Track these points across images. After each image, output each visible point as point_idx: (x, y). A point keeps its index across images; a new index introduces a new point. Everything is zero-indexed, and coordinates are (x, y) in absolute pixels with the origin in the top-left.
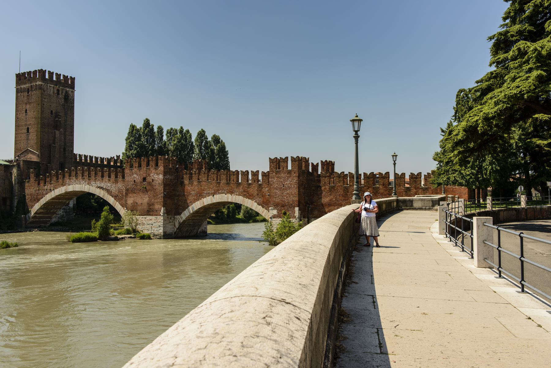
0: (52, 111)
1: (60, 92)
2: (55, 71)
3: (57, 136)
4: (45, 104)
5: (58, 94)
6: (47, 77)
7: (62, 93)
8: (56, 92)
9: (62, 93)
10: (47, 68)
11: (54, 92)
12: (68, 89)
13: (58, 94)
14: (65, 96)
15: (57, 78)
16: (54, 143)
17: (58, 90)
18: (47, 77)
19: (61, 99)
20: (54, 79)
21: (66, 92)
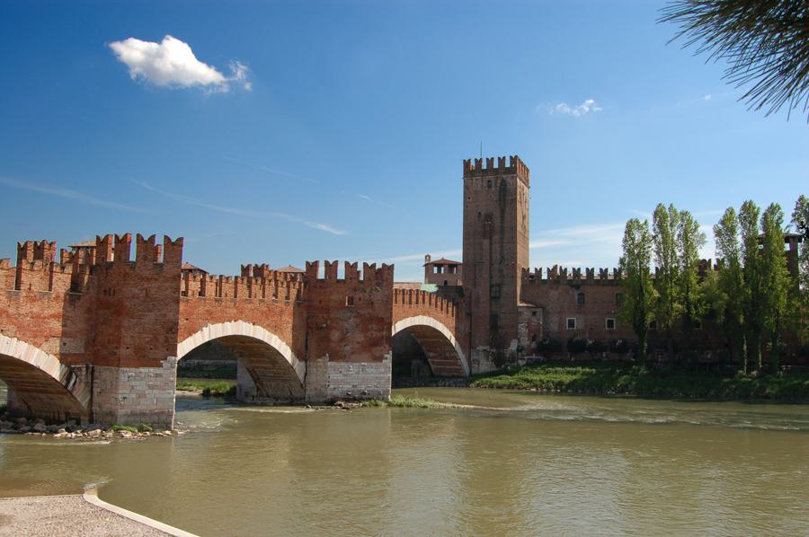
0: (480, 213)
2: (485, 156)
3: (484, 247)
5: (490, 186)
8: (485, 184)
10: (473, 157)
12: (504, 176)
13: (490, 186)
14: (501, 184)
15: (488, 165)
21: (503, 181)
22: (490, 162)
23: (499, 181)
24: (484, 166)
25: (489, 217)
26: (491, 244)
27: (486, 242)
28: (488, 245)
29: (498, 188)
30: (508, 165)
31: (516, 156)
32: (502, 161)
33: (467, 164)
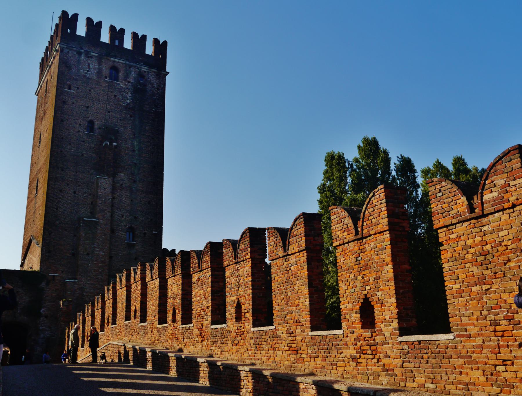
0: (91, 123)
1: (121, 75)
3: (101, 192)
4: (70, 101)
6: (81, 30)
7: (126, 76)
8: (105, 71)
9: (126, 76)
11: (99, 73)
12: (144, 69)
15: (112, 38)
16: (93, 214)
17: (114, 69)
18: (81, 30)
19: (121, 90)
20: (105, 37)
22: (117, 34)
23: (134, 74)
24: (105, 37)
25: (110, 132)
26: (114, 189)
27: (105, 184)
28: (108, 190)
29: (130, 86)
30: (150, 50)
31: (165, 43)
32: (139, 41)
33: (67, 21)
